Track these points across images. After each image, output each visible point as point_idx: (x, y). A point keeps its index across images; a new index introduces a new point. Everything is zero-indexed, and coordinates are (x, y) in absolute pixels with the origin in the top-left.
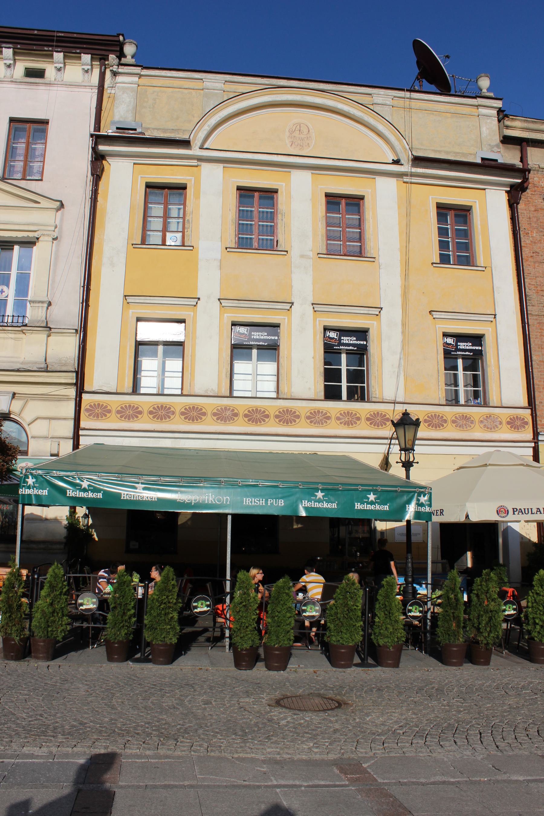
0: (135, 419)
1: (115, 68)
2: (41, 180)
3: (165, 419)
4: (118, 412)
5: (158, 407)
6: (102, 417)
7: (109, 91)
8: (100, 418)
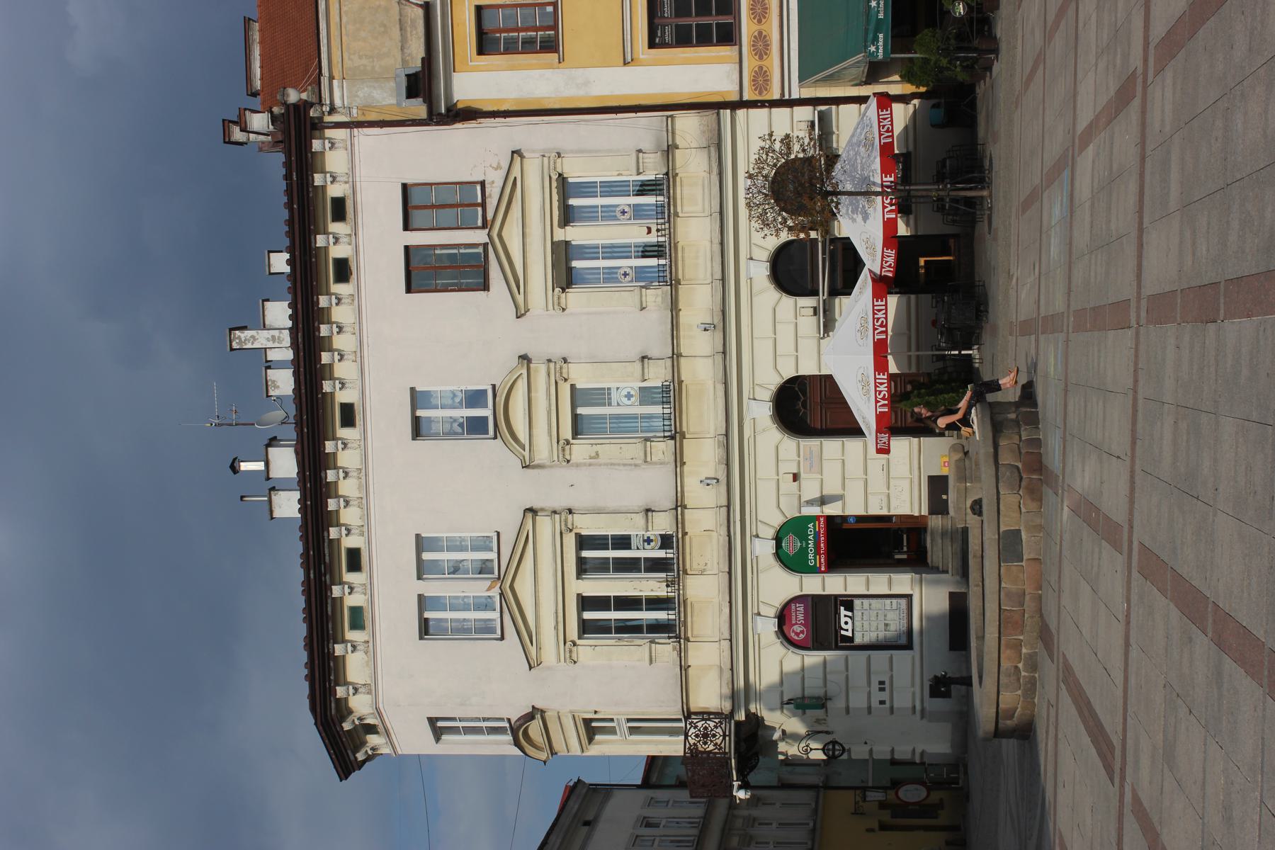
0: (768, 38)
1: (326, 109)
2: (483, 184)
3: (765, 4)
4: (761, 58)
5: (752, 14)
6: (768, 76)
7: (355, 115)
8: (769, 78)
